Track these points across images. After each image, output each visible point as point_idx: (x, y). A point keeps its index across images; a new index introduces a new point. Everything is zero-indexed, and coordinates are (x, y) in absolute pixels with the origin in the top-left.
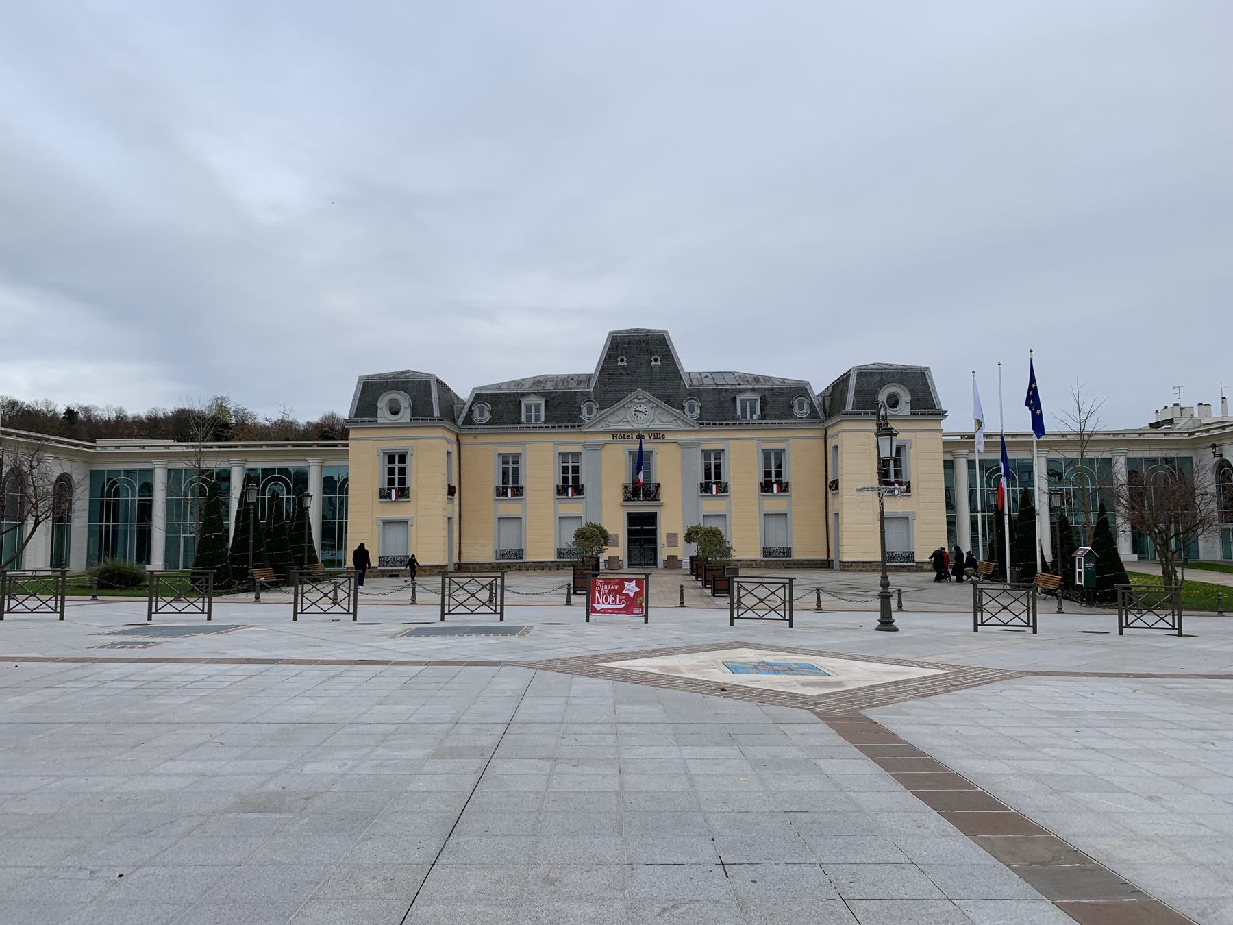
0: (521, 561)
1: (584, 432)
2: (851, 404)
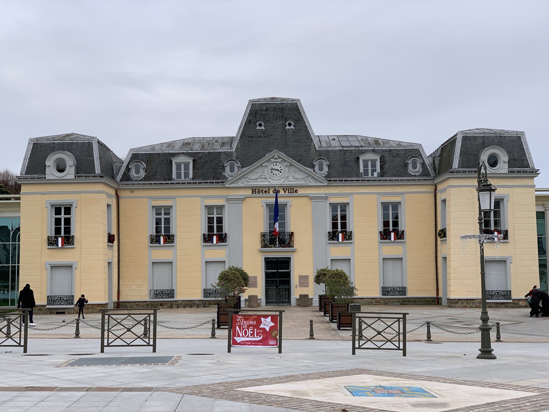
1: (228, 188)
2: (457, 164)
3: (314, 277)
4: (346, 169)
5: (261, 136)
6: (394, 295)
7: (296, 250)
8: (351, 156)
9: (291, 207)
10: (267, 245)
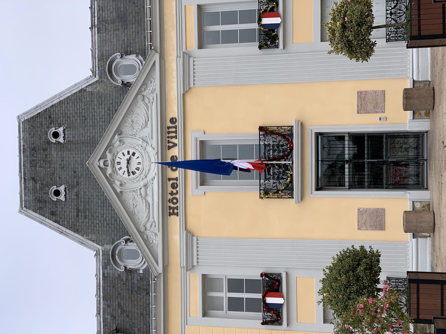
3: (354, 60)
4: (131, 16)
5: (76, 192)
8: (109, 7)
9: (206, 132)
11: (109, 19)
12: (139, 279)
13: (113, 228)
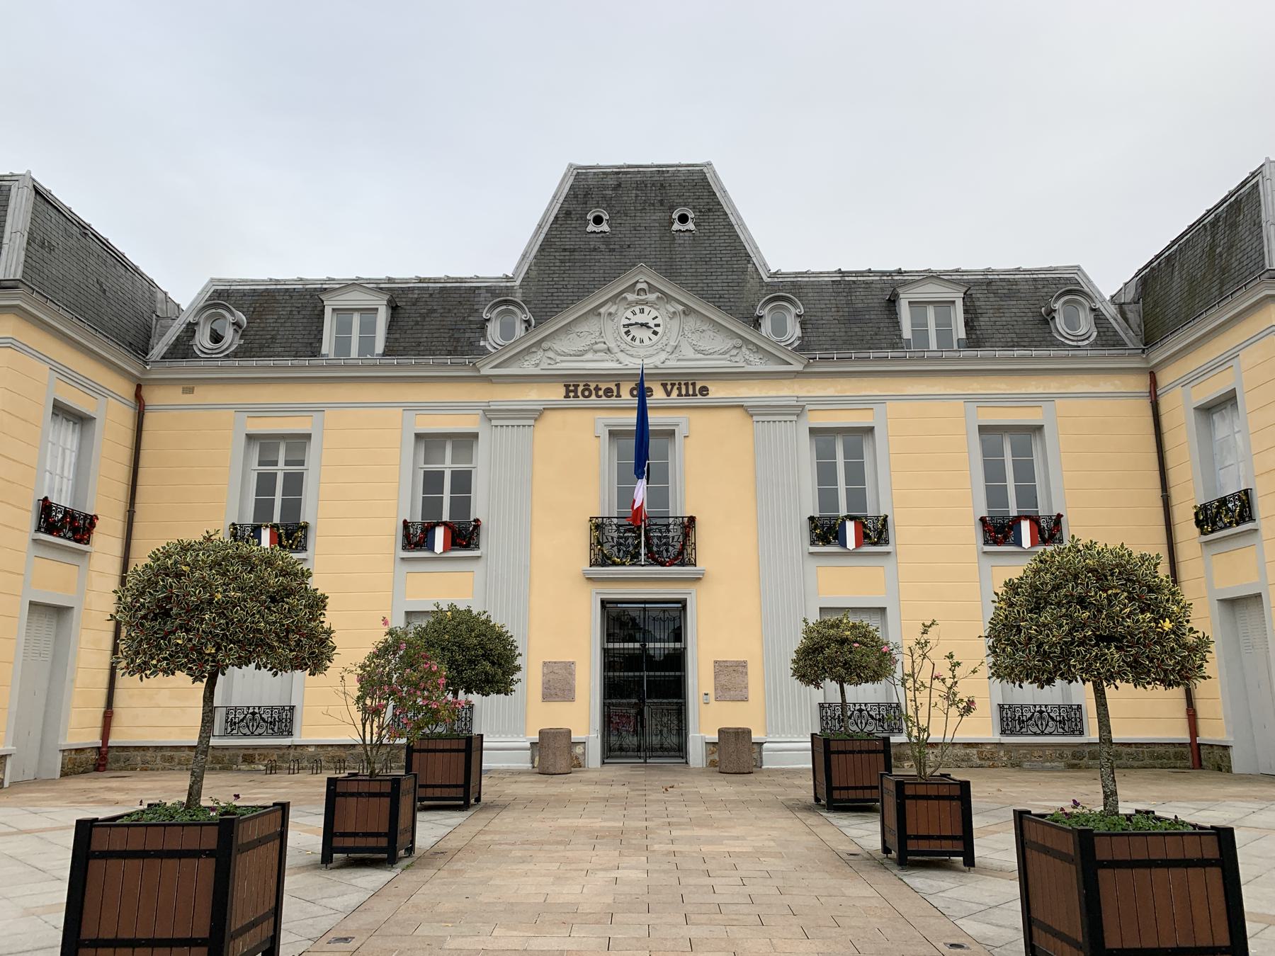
0: (286, 741)
3: (794, 656)
4: (857, 330)
6: (1042, 732)
7: (703, 574)
8: (870, 297)
9: (686, 439)
10: (609, 559)
11: (853, 298)
12: (472, 340)
13: (546, 302)
